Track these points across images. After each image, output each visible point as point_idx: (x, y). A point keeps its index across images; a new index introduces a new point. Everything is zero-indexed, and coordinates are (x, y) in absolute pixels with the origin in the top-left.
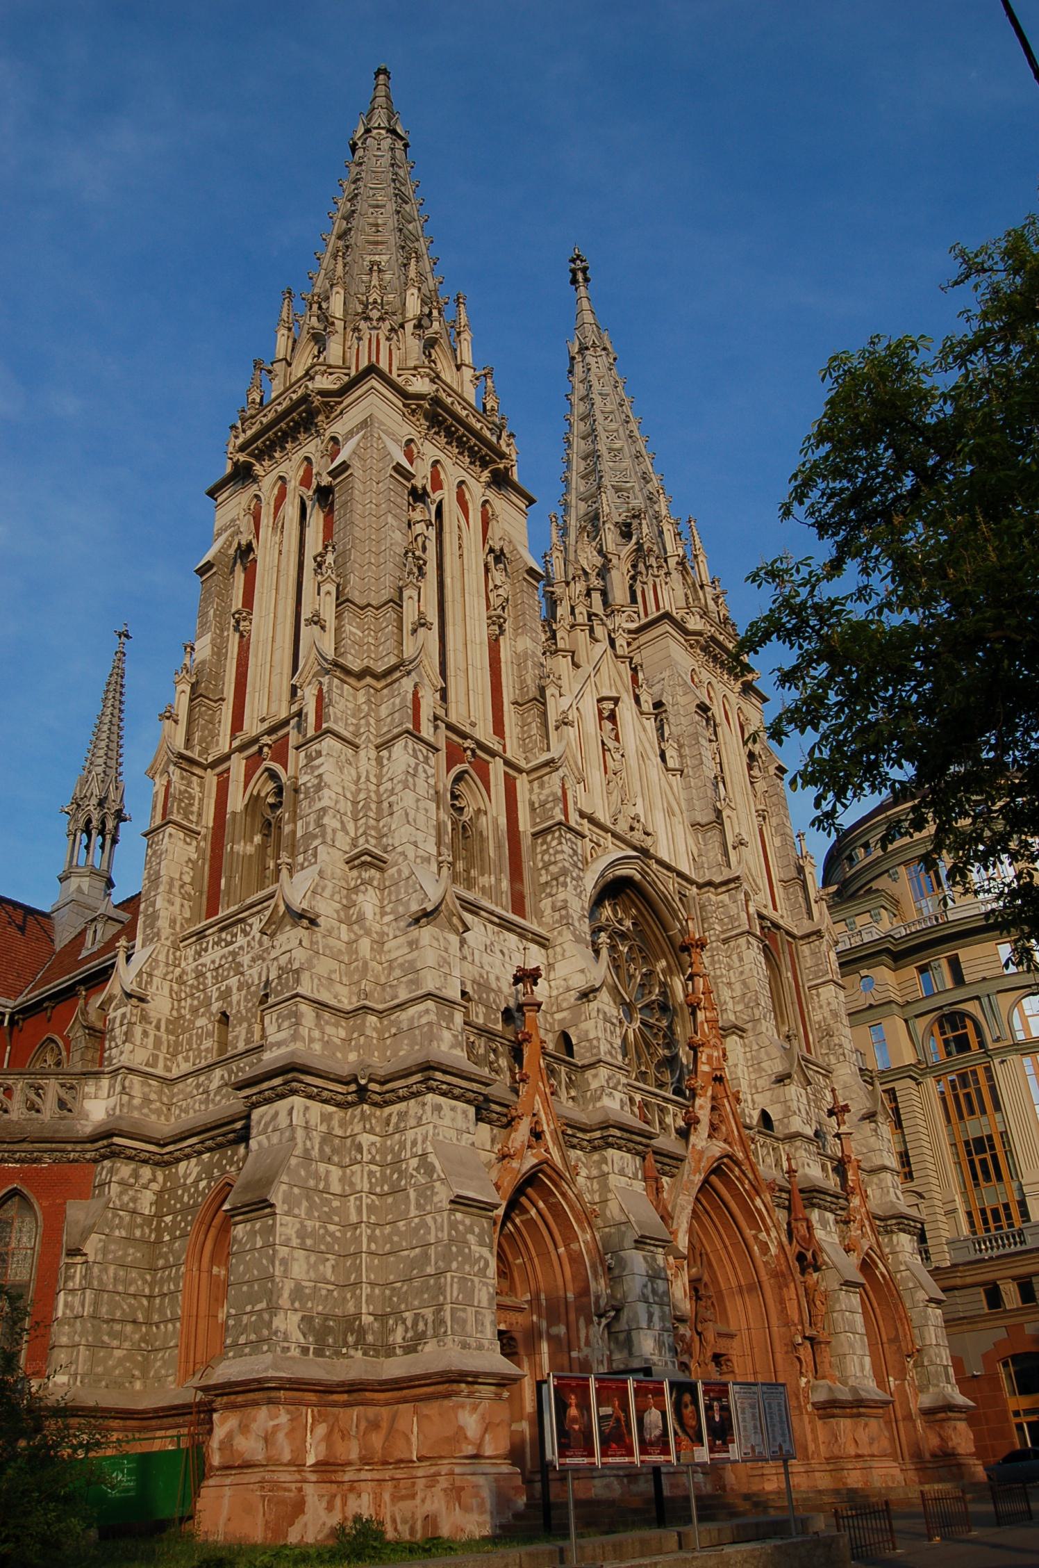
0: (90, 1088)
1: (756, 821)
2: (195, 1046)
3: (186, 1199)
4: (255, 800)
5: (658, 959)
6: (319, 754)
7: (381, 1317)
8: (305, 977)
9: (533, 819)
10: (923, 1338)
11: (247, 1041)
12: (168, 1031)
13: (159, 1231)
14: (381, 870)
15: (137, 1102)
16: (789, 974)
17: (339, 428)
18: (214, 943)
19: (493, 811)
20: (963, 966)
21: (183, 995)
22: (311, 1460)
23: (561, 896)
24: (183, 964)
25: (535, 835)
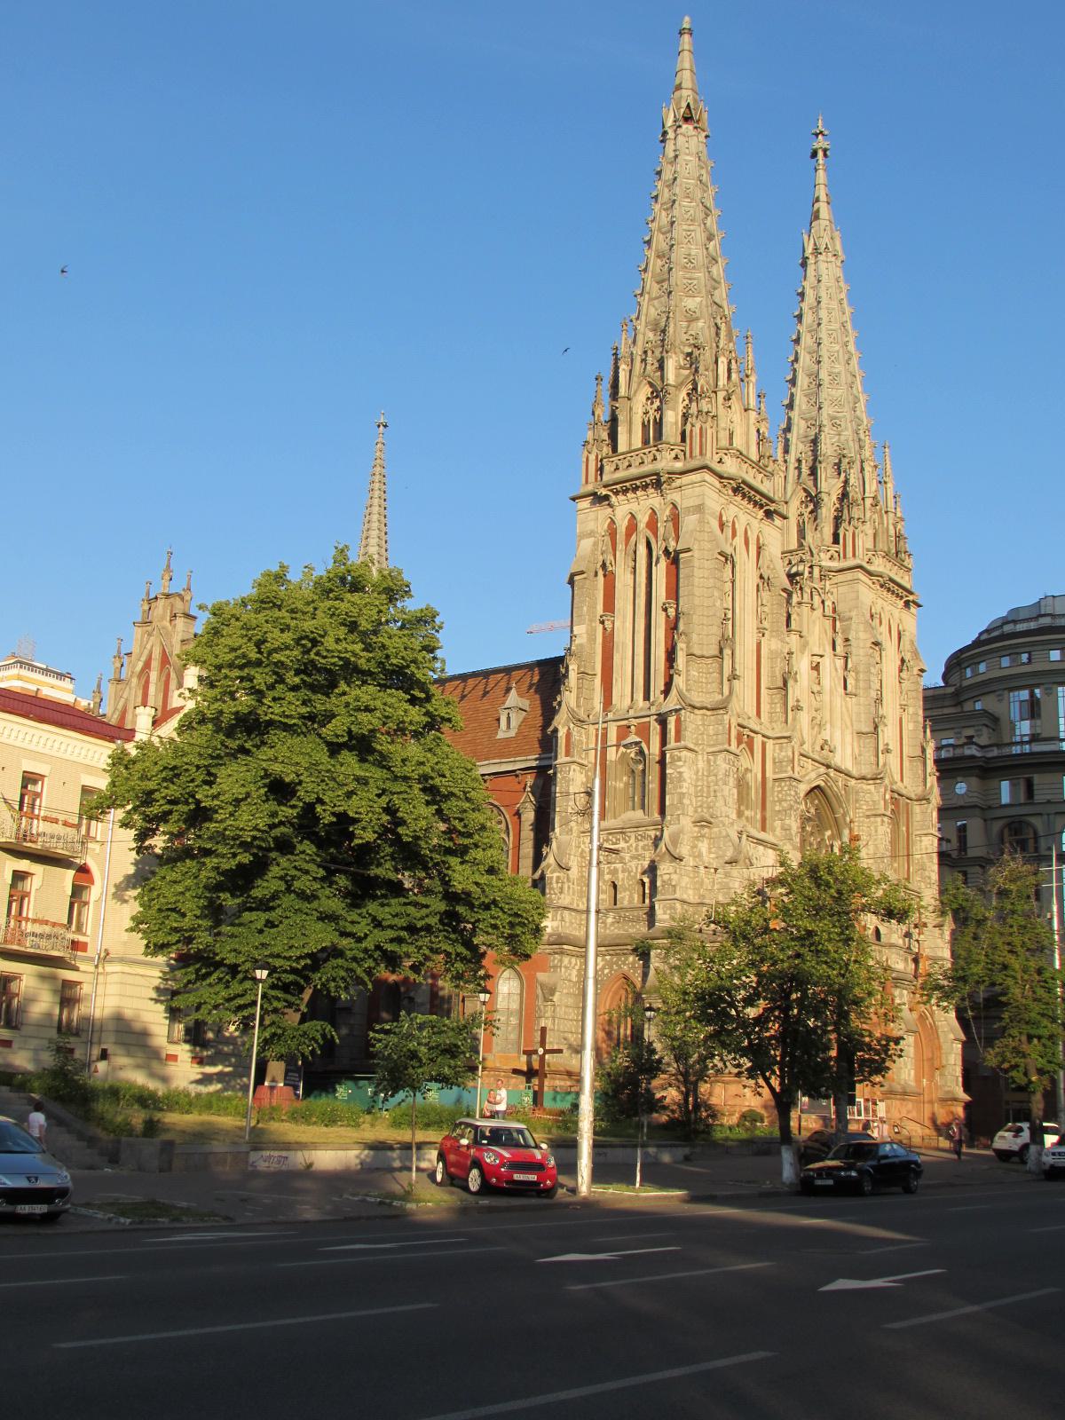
1: (899, 711)
5: (827, 830)
6: (679, 759)
8: (678, 888)
9: (774, 769)
10: (947, 1060)
11: (630, 902)
16: (904, 829)
19: (754, 771)
20: (1035, 787)
23: (787, 822)
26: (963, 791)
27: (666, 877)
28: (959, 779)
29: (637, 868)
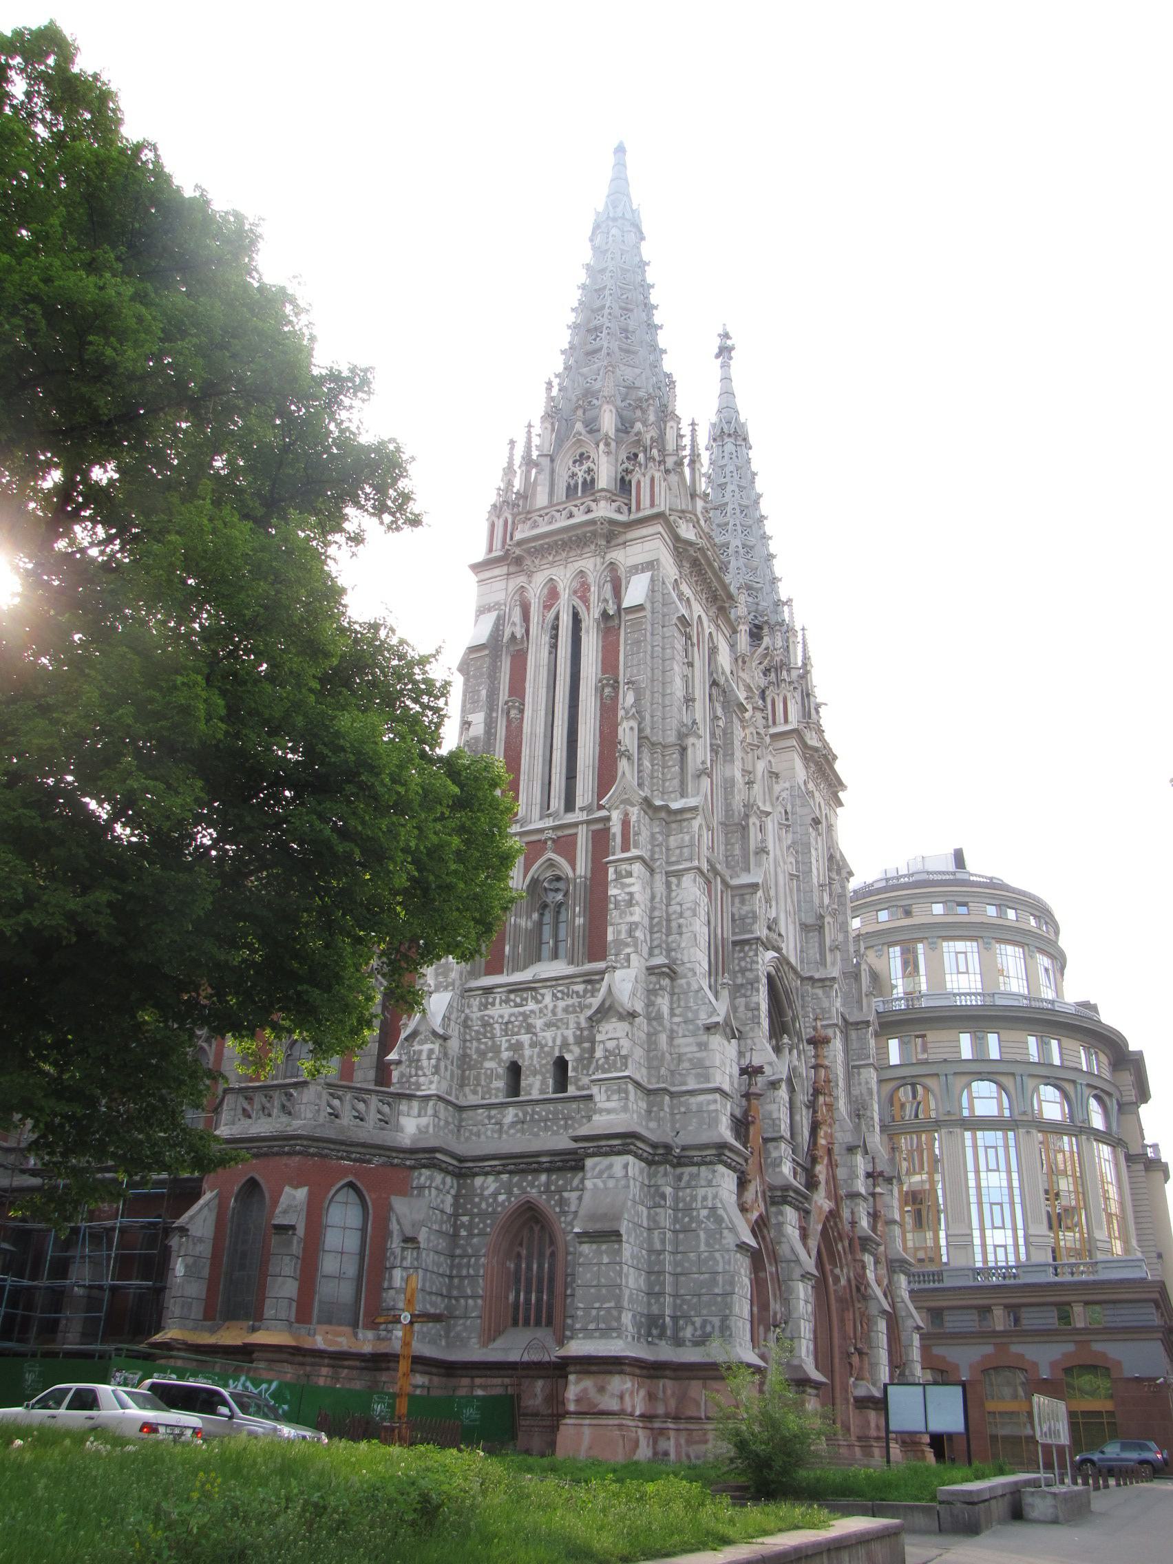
0: (404, 1107)
2: (483, 1083)
3: (484, 1206)
4: (535, 883)
6: (630, 874)
7: (675, 1318)
9: (733, 929)
10: (907, 1355)
11: (542, 1092)
12: (458, 1067)
13: (456, 1228)
14: (672, 979)
15: (442, 1123)
17: (618, 555)
18: (501, 1001)
21: (468, 1037)
22: (637, 1413)
23: (754, 999)
24: (467, 1011)
25: (735, 943)
27: (611, 1045)
29: (554, 1041)
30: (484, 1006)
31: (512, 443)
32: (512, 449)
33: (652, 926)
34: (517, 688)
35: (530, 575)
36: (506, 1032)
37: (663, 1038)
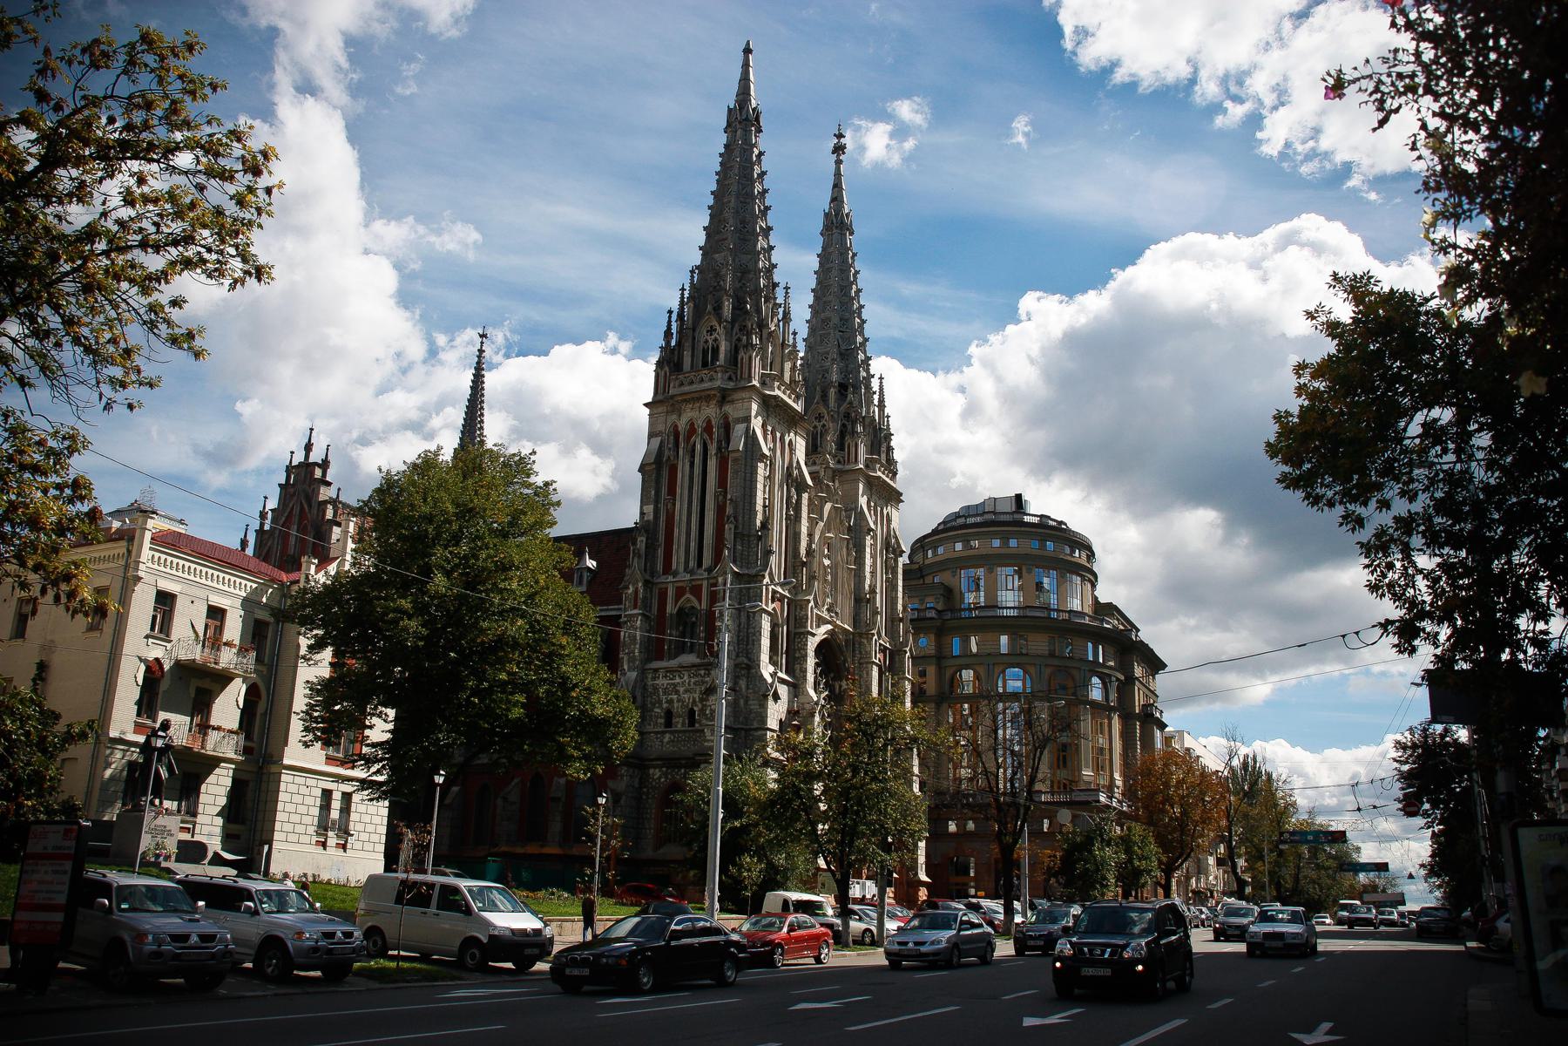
4: (681, 610)
17: (728, 408)
26: (925, 644)
28: (922, 635)
30: (654, 679)
31: (670, 312)
32: (670, 317)
33: (738, 640)
34: (672, 491)
35: (680, 416)
36: (665, 693)
37: (742, 702)
